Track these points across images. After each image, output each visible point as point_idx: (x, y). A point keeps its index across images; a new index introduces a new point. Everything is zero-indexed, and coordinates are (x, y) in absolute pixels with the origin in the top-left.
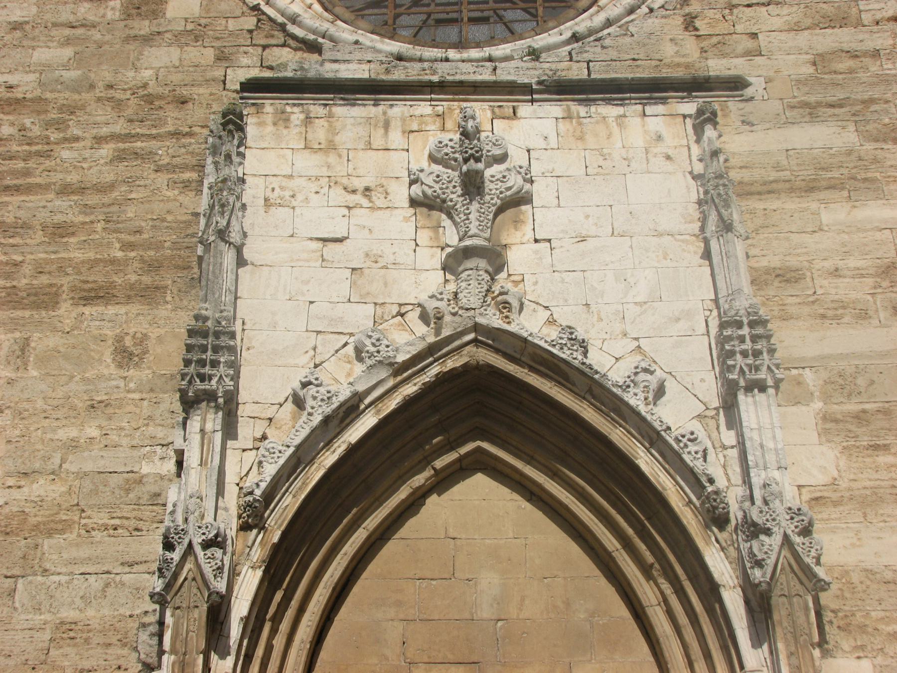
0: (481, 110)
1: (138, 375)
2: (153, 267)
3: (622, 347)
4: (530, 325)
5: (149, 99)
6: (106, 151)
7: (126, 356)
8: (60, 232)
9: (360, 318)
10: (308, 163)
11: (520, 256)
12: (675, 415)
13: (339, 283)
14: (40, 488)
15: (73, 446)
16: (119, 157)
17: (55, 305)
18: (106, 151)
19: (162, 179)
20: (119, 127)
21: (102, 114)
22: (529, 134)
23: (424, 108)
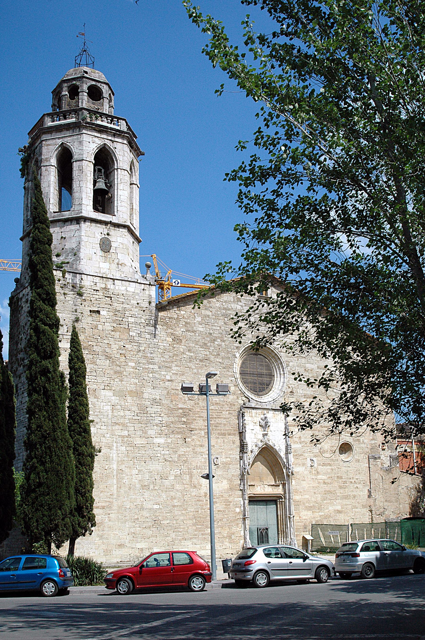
0: (265, 412)
1: (235, 446)
2: (235, 430)
3: (278, 445)
4: (271, 443)
5: (231, 404)
6: (227, 412)
7: (234, 443)
8: (225, 425)
9: (255, 440)
10: (250, 419)
11: (269, 433)
12: (282, 454)
13: (253, 436)
14: (228, 459)
15: (230, 454)
16: (229, 413)
17: (225, 435)
18: (227, 412)
19: (234, 417)
20: (228, 409)
21: (226, 406)
22: (270, 415)
23: (260, 411)
